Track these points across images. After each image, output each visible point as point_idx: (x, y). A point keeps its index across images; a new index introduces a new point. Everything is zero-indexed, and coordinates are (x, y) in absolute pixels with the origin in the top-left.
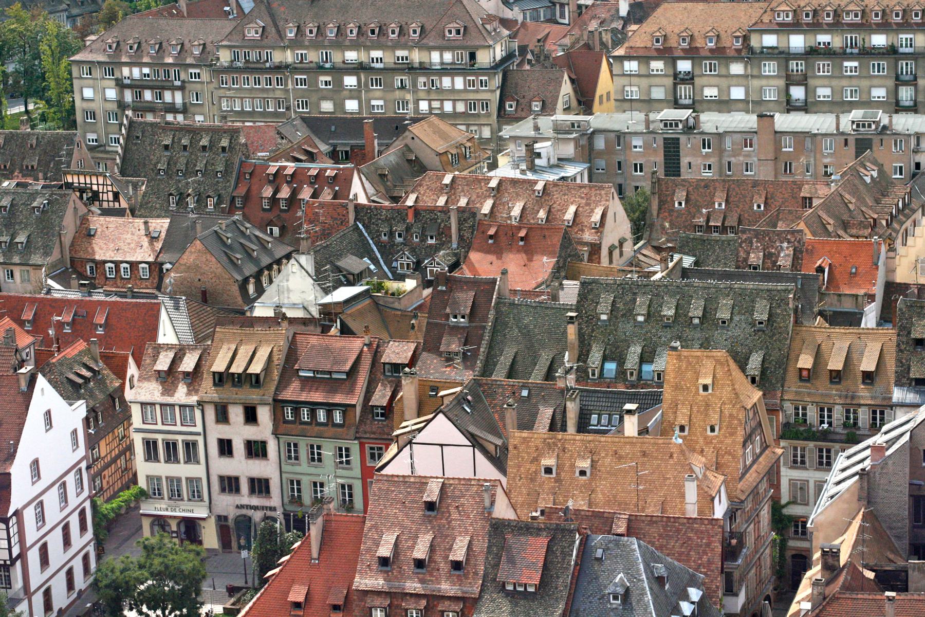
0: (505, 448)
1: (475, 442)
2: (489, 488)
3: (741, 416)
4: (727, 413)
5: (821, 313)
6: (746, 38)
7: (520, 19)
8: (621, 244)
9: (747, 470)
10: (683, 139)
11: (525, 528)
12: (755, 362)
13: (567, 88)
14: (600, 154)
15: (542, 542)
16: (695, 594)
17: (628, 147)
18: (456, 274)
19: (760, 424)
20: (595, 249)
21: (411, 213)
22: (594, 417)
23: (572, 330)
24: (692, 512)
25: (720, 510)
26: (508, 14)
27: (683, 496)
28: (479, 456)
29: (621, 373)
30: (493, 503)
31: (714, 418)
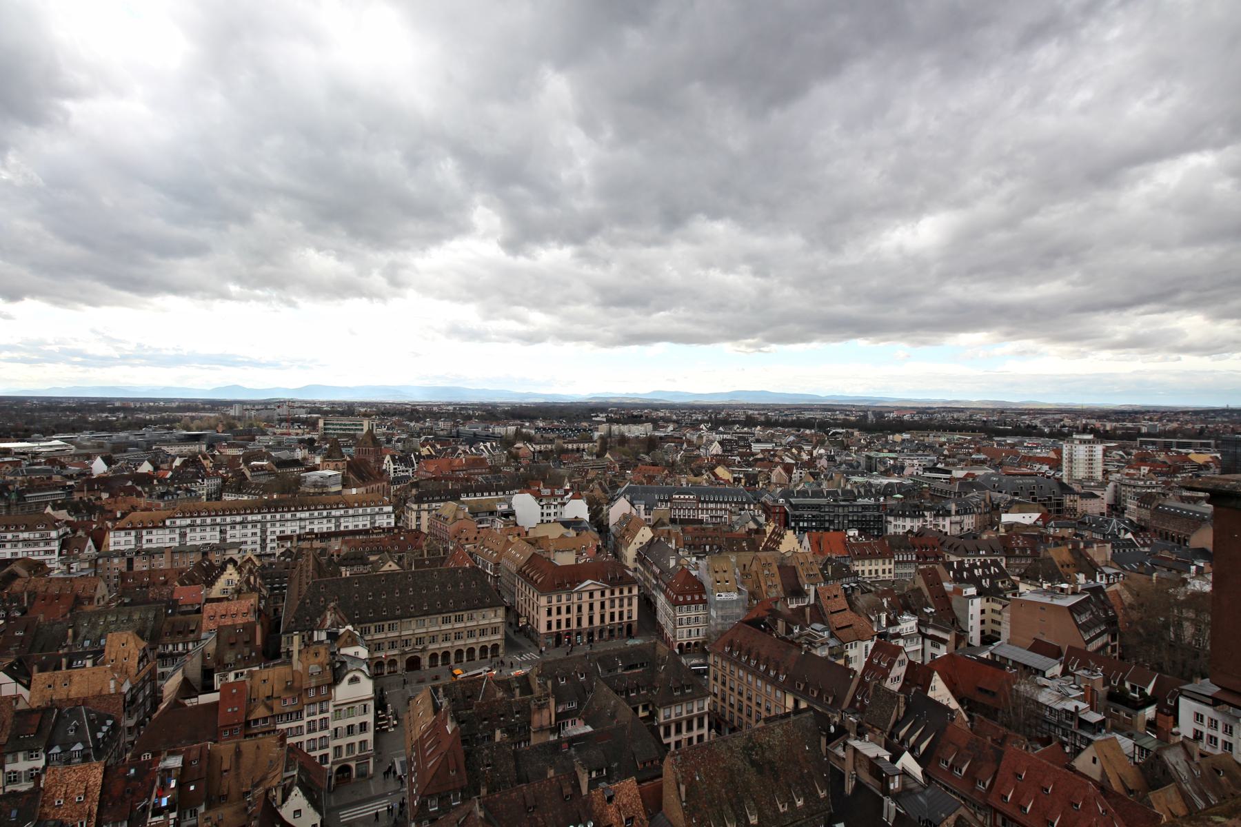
0: (30, 682)
1: (17, 681)
2: (17, 698)
3: (138, 652)
4: (131, 652)
5: (179, 613)
6: (164, 522)
7: (76, 520)
8: (103, 597)
9: (139, 671)
10: (135, 558)
11: (31, 712)
12: (148, 634)
13: (90, 543)
14: (100, 565)
15: (40, 715)
16: (109, 722)
17: (112, 562)
18: (25, 616)
19: (146, 655)
20: (91, 599)
21: (5, 595)
22: (75, 663)
23: (70, 631)
24: (112, 691)
25: (126, 688)
26: (71, 519)
27: (109, 686)
28: (19, 685)
29: (92, 644)
30: (17, 703)
31: (126, 655)
